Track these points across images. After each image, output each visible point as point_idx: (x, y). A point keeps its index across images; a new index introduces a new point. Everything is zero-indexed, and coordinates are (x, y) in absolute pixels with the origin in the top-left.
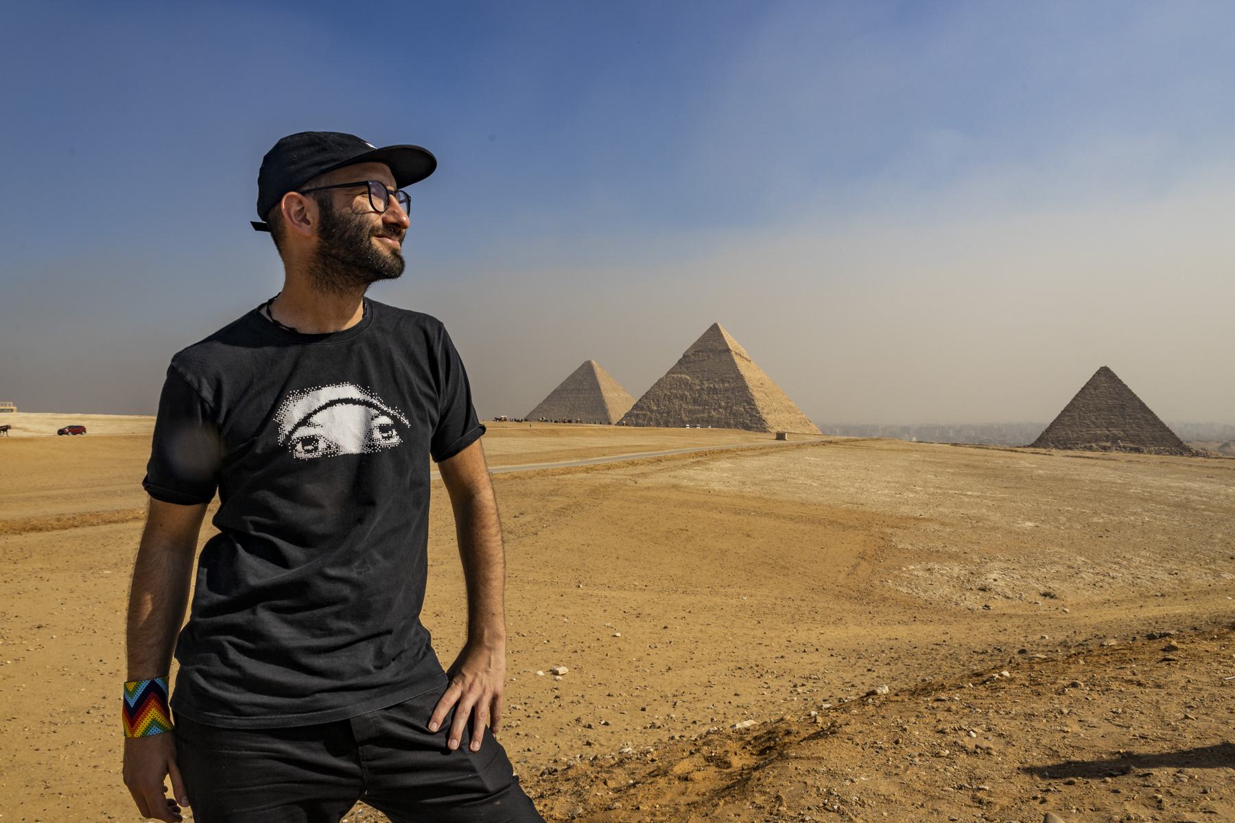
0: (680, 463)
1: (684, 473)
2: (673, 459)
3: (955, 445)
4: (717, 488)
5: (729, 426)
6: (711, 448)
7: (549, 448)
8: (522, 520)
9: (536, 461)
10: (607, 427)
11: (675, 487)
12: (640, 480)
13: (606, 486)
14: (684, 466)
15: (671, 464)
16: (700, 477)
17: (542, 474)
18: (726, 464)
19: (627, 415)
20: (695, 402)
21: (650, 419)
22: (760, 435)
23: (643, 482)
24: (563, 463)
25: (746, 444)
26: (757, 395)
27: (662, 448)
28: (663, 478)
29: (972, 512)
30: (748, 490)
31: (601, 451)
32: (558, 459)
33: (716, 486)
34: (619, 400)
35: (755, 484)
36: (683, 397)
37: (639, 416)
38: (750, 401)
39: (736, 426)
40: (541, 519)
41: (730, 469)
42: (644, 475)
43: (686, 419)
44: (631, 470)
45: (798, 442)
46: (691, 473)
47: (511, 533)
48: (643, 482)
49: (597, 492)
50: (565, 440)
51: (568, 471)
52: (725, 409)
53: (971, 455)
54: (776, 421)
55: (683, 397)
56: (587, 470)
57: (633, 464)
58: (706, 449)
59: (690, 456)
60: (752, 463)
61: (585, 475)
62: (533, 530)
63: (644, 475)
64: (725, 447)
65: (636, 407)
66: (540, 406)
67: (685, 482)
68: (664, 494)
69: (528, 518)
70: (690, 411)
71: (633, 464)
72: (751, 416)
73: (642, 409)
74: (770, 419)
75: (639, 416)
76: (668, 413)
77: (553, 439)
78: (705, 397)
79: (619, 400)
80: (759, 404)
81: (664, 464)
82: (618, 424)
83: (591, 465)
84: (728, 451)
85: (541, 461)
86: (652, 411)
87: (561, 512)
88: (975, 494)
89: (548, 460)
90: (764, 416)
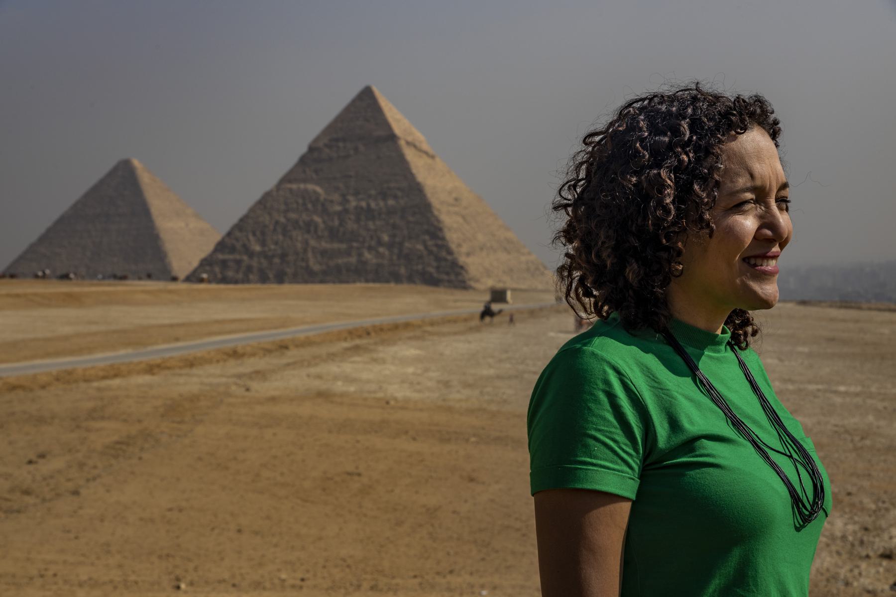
0: (323, 350)
1: (333, 368)
2: (307, 343)
3: (803, 303)
4: (399, 395)
5: (397, 278)
6: (377, 320)
7: (67, 330)
8: (45, 467)
9: (48, 355)
10: (172, 286)
11: (324, 395)
12: (255, 385)
13: (194, 398)
14: (331, 357)
15: (306, 353)
16: (365, 376)
17: (66, 378)
18: (409, 350)
19: (206, 263)
20: (333, 234)
21: (249, 269)
22: (459, 295)
23: (260, 388)
24: (101, 358)
25: (437, 313)
26: (448, 219)
27: (284, 323)
28: (296, 380)
29: (852, 421)
30: (458, 396)
31: (172, 332)
32: (90, 350)
33: (398, 392)
34: (187, 233)
35: (467, 385)
36: (309, 227)
37: (235, 261)
38: (435, 231)
39: (410, 279)
40: (81, 465)
41: (417, 360)
42: (260, 375)
43: (316, 268)
44: (233, 367)
45: (532, 305)
46: (347, 368)
47: (27, 492)
48: (260, 388)
49: (176, 410)
50: (95, 313)
51: (115, 372)
52: (390, 246)
53: (832, 320)
54: (483, 267)
55: (309, 227)
56: (151, 369)
57: (235, 354)
58: (367, 322)
59: (340, 336)
60: (457, 347)
61: (147, 378)
62: (70, 486)
63: (260, 375)
64: (401, 319)
65: (221, 246)
66: (32, 249)
67: (339, 386)
68: (306, 409)
69: (56, 464)
70: (324, 253)
71: (235, 354)
72: (438, 259)
73: (233, 250)
74: (473, 264)
75: (235, 261)
76: (283, 256)
77: (71, 313)
78: (351, 225)
79: (187, 233)
80: (452, 237)
81: (293, 354)
82: (194, 278)
83: (156, 359)
84: (407, 326)
85: (58, 354)
86: (251, 254)
87: (118, 449)
88: (852, 389)
89: (72, 353)
90: (462, 260)
